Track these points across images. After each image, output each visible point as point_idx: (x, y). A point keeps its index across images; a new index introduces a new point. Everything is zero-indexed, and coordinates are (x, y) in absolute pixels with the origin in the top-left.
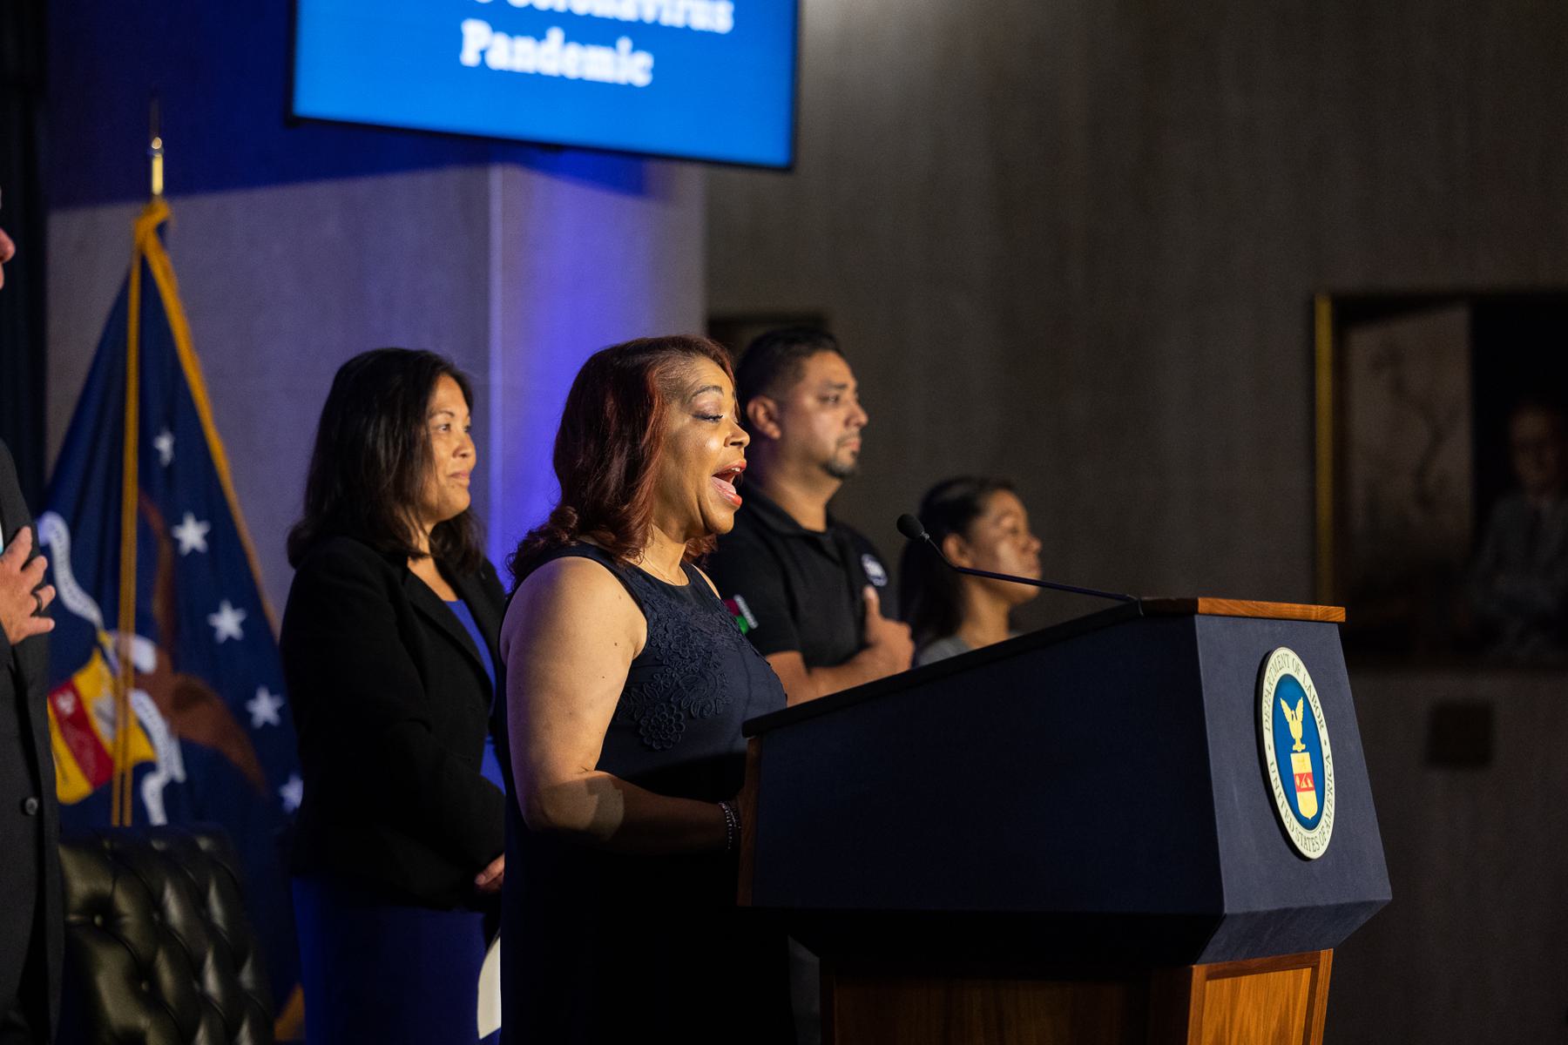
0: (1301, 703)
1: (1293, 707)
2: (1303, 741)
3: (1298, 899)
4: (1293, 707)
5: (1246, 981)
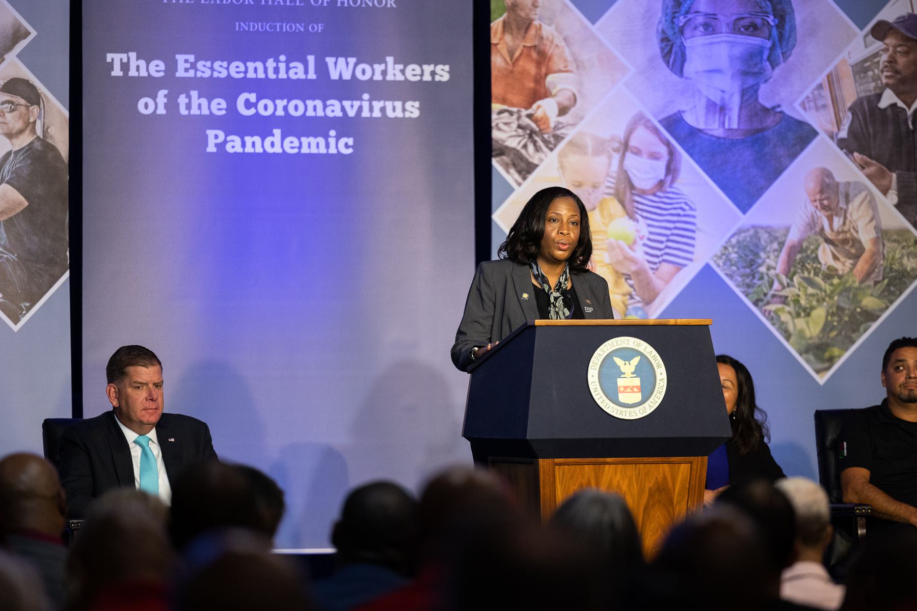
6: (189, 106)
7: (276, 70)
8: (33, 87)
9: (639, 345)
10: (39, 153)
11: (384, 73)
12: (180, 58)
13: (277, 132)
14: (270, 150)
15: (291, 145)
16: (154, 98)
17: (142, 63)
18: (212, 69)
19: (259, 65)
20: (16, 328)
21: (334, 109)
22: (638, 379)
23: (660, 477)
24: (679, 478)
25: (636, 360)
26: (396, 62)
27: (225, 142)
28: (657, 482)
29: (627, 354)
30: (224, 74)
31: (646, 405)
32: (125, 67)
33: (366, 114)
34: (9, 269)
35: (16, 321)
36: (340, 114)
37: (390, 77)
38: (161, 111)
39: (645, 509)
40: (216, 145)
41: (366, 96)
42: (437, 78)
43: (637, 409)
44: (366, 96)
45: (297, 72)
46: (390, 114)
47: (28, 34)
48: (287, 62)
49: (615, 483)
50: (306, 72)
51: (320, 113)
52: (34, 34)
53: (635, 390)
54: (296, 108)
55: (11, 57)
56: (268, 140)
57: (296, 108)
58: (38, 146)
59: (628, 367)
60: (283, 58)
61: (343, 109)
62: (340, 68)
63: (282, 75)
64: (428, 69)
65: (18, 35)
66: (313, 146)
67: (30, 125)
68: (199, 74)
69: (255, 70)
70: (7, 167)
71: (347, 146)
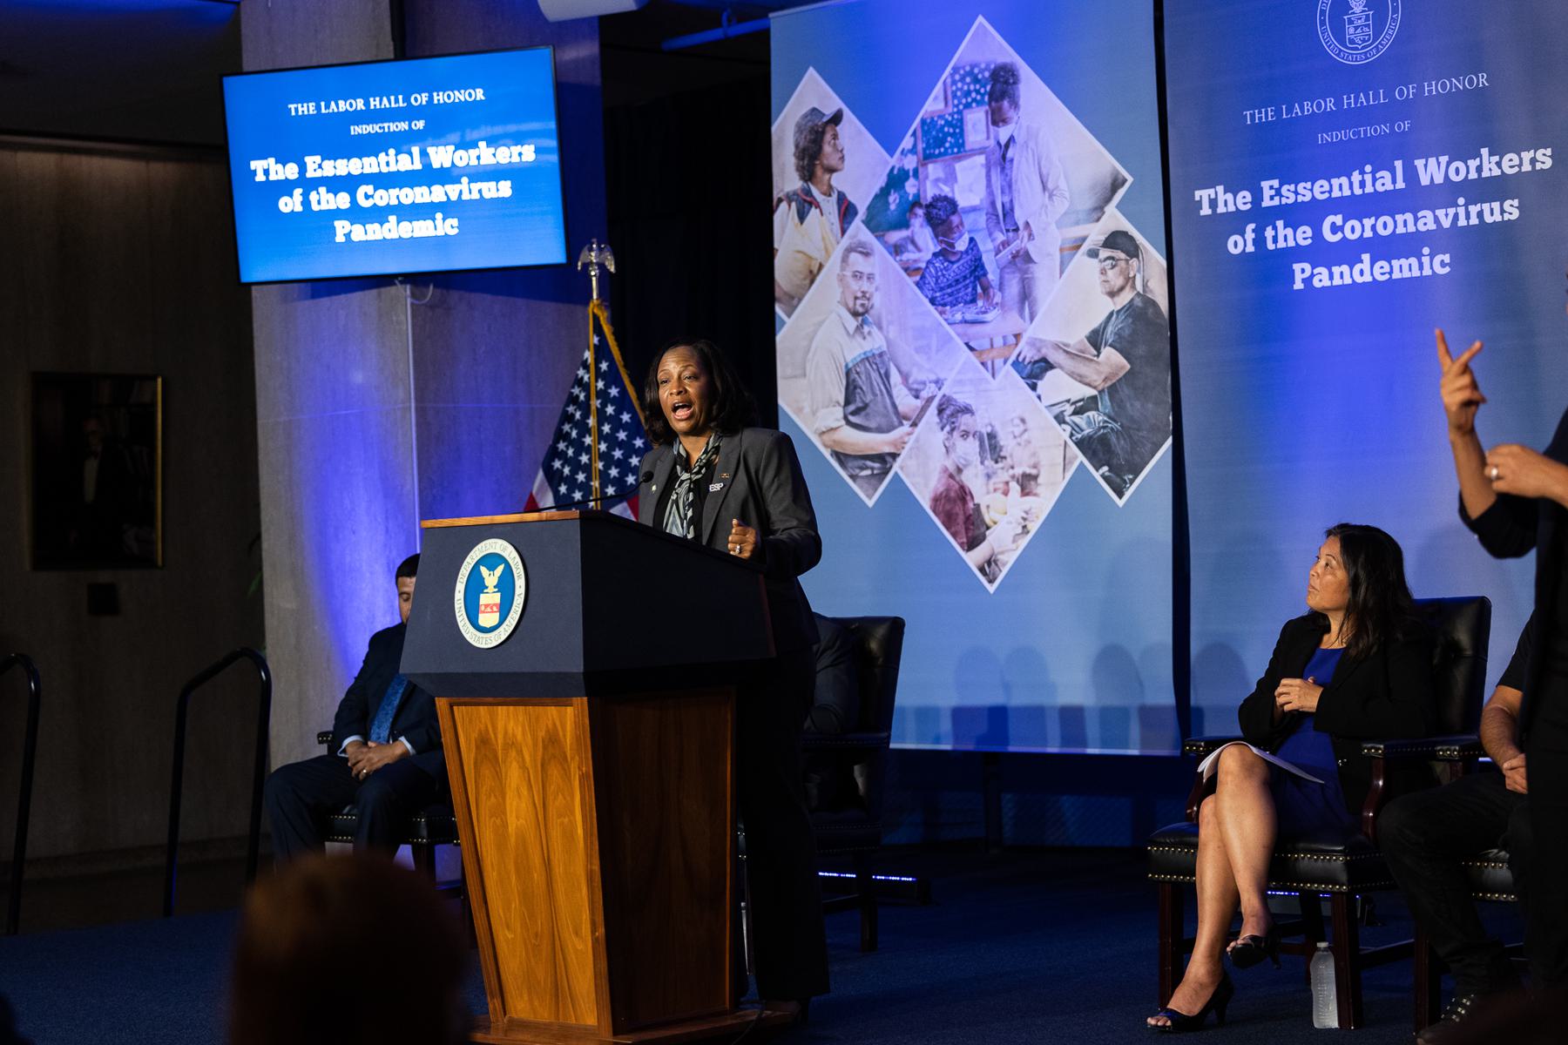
1: (492, 568)
3: (454, 667)
5: (501, 710)
6: (1275, 240)
7: (1362, 184)
8: (1131, 238)
10: (1139, 312)
11: (1479, 169)
12: (1265, 184)
13: (1366, 257)
14: (1359, 280)
15: (1381, 271)
16: (1243, 234)
17: (1229, 196)
18: (1296, 193)
19: (1344, 180)
20: (1121, 503)
21: (1427, 221)
24: (568, 728)
25: (501, 568)
26: (1491, 154)
27: (1313, 275)
28: (548, 731)
29: (492, 560)
30: (1307, 199)
32: (1213, 203)
33: (1462, 222)
34: (1113, 439)
35: (1120, 495)
36: (1432, 226)
37: (1485, 174)
38: (1250, 248)
40: (1304, 280)
41: (1461, 201)
42: (1539, 166)
43: (492, 634)
44: (1461, 201)
45: (1385, 182)
46: (1488, 219)
47: (1125, 181)
48: (1373, 173)
50: (1394, 181)
51: (1411, 228)
52: (1130, 180)
54: (1385, 226)
55: (1111, 209)
56: (1357, 267)
57: (1385, 226)
58: (1138, 303)
59: (491, 578)
60: (1368, 168)
61: (1437, 220)
62: (1432, 171)
63: (1369, 189)
64: (1527, 156)
65: (1116, 183)
66: (1405, 268)
67: (1129, 281)
68: (1284, 201)
69: (1341, 187)
70: (1110, 329)
71: (1443, 264)
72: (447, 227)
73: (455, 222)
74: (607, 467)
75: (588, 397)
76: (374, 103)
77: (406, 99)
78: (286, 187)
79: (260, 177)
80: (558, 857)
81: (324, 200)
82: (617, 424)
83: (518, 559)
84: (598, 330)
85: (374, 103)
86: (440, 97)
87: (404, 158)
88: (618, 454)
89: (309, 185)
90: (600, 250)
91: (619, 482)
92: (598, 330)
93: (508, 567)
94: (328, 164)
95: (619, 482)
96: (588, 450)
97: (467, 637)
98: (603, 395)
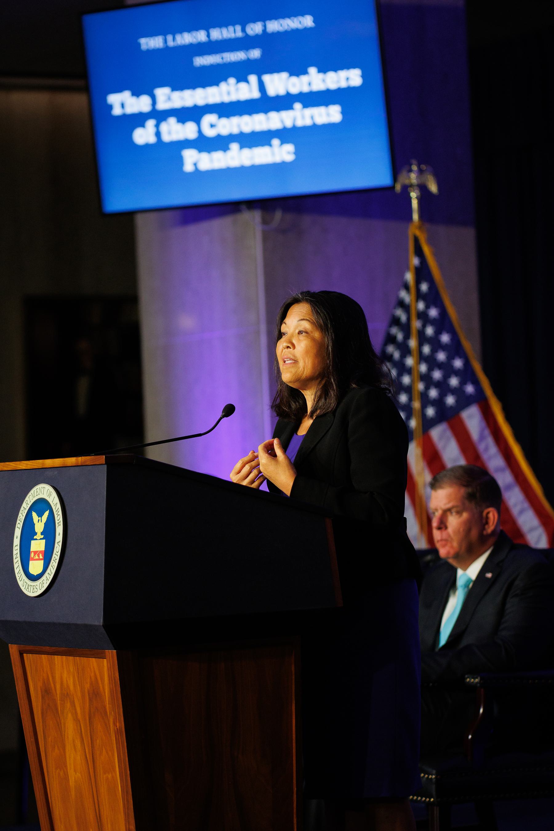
0: (47, 513)
1: (40, 515)
2: (42, 534)
4: (40, 515)
5: (57, 659)
9: (50, 495)
22: (44, 540)
23: (93, 678)
28: (91, 684)
29: (41, 505)
31: (44, 578)
39: (90, 718)
49: (65, 682)
53: (41, 557)
72: (284, 153)
73: (289, 148)
74: (427, 388)
75: (409, 319)
76: (216, 34)
77: (243, 30)
78: (139, 120)
79: (117, 111)
80: (106, 813)
81: (173, 131)
82: (436, 345)
83: (59, 506)
84: (419, 252)
85: (216, 34)
86: (273, 26)
87: (243, 85)
88: (437, 375)
89: (160, 116)
90: (421, 172)
91: (439, 403)
92: (419, 252)
93: (52, 514)
94: (176, 95)
95: (439, 403)
96: (409, 371)
97: (20, 584)
98: (423, 316)
